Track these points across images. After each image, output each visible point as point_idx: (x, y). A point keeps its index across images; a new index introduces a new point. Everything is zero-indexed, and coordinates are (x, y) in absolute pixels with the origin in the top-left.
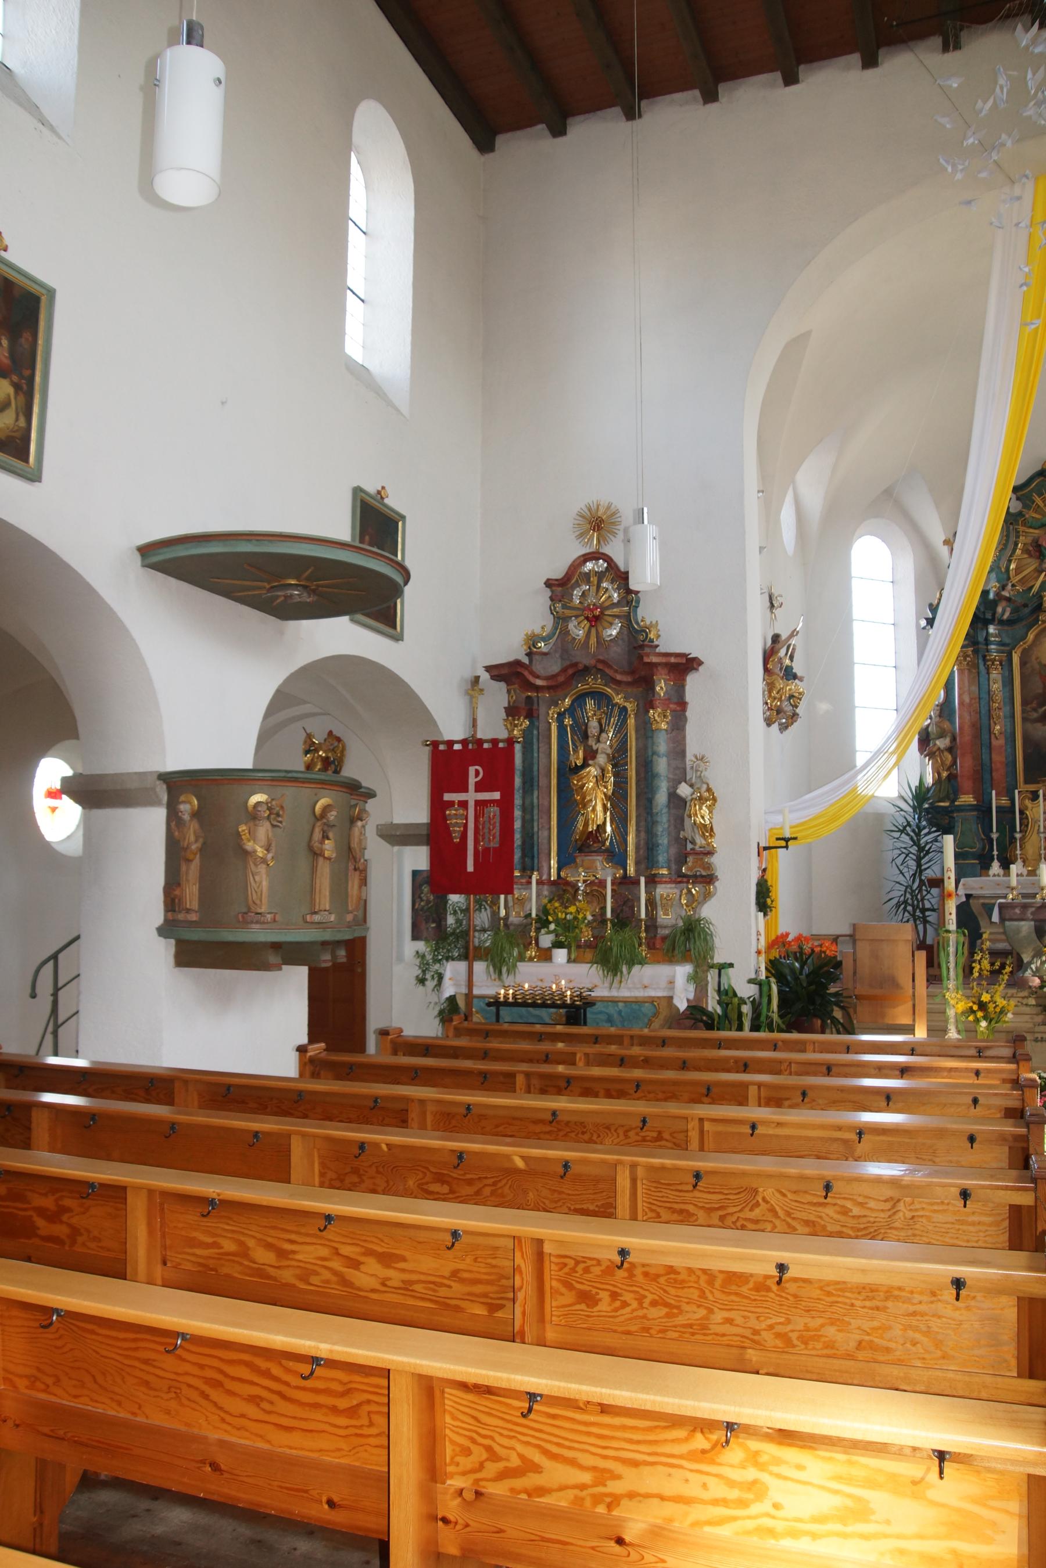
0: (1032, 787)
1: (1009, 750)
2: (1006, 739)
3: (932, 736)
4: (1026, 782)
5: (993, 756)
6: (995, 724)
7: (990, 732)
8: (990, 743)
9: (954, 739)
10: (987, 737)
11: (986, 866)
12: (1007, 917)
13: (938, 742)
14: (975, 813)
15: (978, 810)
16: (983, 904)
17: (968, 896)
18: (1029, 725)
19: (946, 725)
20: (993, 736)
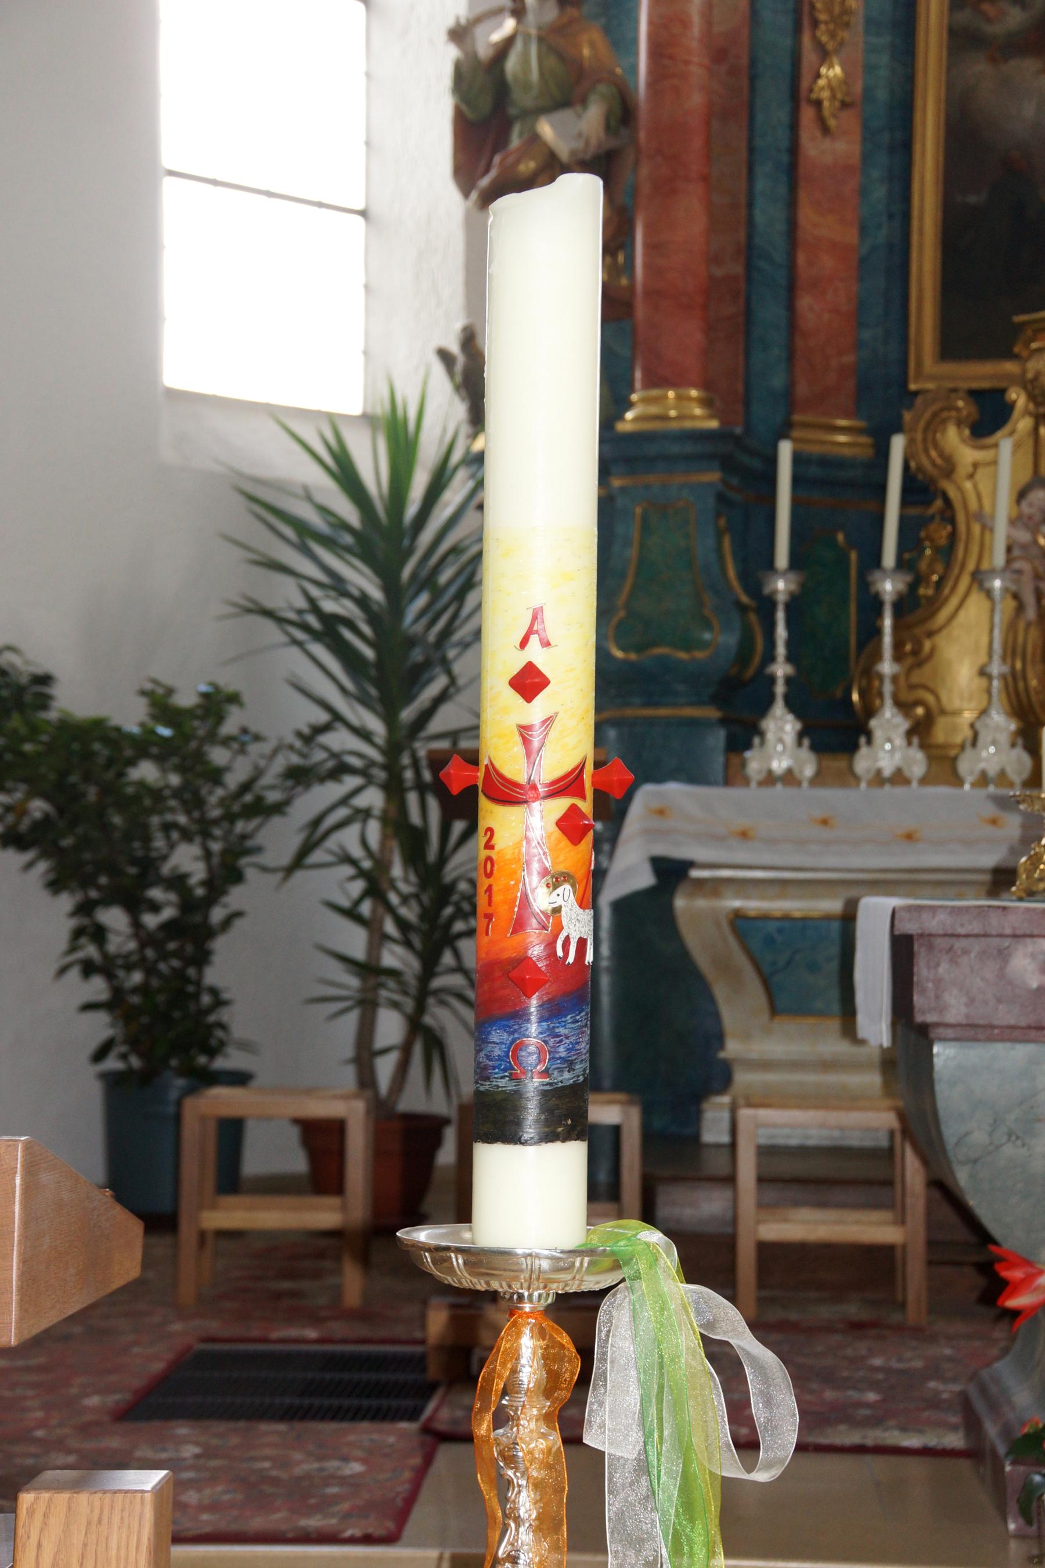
0: (981, 373)
1: (880, 192)
2: (869, 135)
3: (522, 100)
4: (950, 348)
5: (807, 215)
6: (824, 55)
7: (795, 96)
8: (794, 149)
9: (623, 114)
10: (781, 115)
11: (744, 734)
12: (955, 1008)
13: (546, 129)
14: (713, 476)
15: (727, 464)
16: (739, 921)
17: (671, 873)
18: (978, 66)
19: (590, 46)
20: (807, 114)
